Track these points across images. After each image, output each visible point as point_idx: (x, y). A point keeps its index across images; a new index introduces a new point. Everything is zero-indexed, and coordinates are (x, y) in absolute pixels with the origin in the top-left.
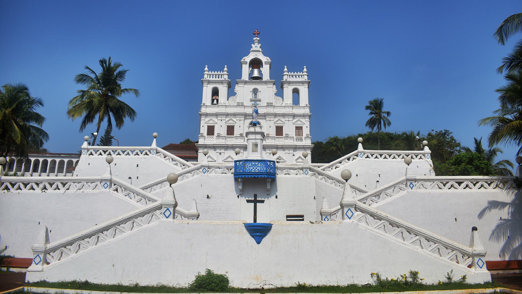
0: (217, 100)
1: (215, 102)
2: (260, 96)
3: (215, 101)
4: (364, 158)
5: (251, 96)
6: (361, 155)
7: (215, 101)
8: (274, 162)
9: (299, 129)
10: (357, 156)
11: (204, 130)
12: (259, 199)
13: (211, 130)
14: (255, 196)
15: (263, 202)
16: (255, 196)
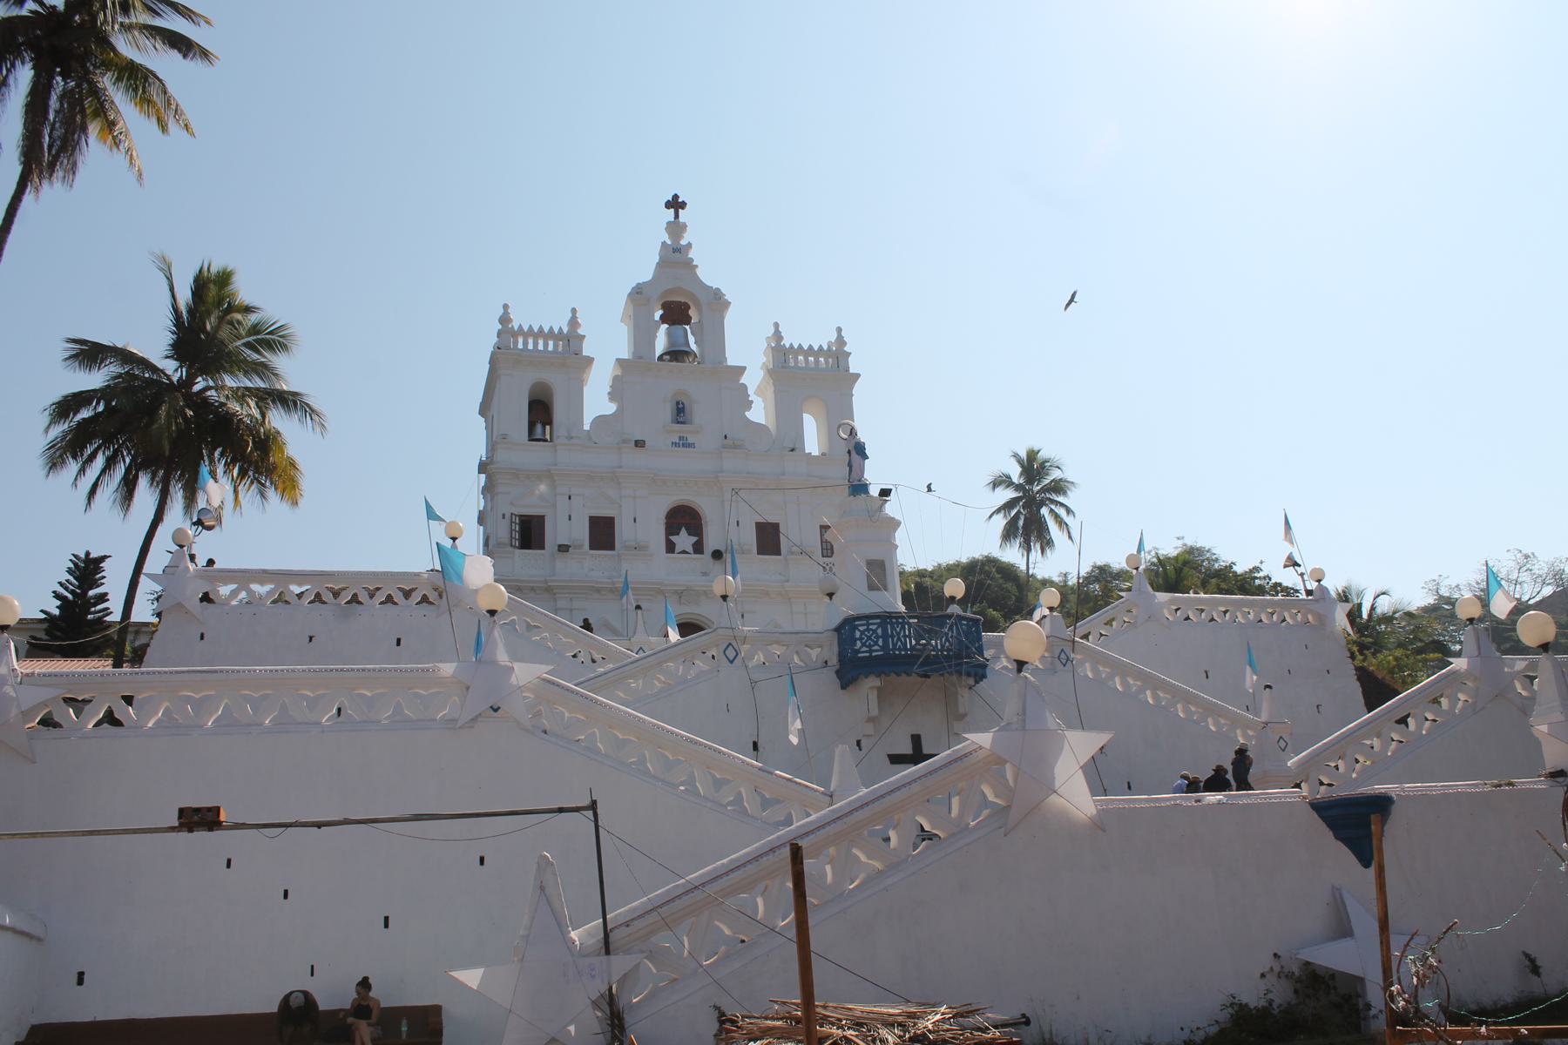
2: (699, 414)
5: (667, 412)
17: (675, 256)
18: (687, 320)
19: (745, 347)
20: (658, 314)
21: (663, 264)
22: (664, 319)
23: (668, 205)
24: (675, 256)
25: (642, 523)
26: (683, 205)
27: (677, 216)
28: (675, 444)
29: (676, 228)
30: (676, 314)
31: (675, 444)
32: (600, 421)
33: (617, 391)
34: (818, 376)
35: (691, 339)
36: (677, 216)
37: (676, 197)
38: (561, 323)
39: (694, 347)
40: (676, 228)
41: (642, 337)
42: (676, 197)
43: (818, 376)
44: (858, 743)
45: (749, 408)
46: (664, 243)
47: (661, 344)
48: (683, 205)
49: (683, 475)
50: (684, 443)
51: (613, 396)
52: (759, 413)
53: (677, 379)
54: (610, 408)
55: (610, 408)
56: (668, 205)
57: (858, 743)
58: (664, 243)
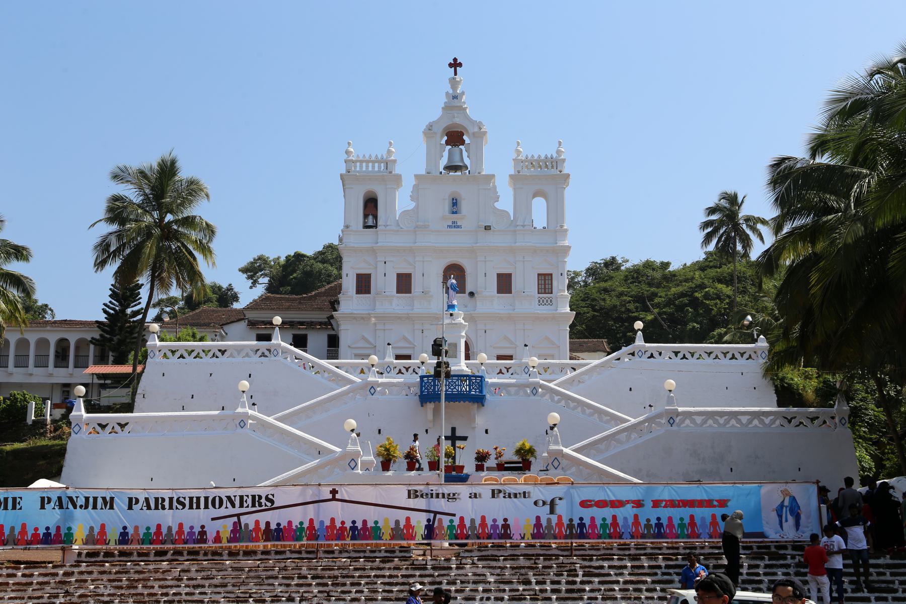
0: (375, 217)
1: (370, 221)
2: (464, 207)
3: (371, 217)
4: (644, 358)
6: (640, 354)
7: (371, 217)
8: (481, 377)
9: (545, 282)
10: (633, 354)
11: (349, 283)
12: (458, 434)
13: (364, 284)
14: (454, 430)
15: (464, 438)
16: (454, 430)
17: (454, 101)
18: (463, 142)
19: (496, 159)
20: (443, 142)
21: (447, 108)
22: (447, 143)
23: (450, 65)
24: (454, 101)
25: (428, 278)
26: (460, 65)
27: (456, 74)
28: (449, 226)
29: (454, 83)
30: (455, 138)
31: (449, 226)
32: (405, 213)
33: (415, 195)
34: (544, 176)
35: (465, 154)
36: (456, 74)
37: (455, 60)
38: (381, 153)
39: (467, 161)
40: (454, 83)
41: (431, 159)
42: (455, 60)
43: (544, 176)
44: (427, 431)
45: (497, 199)
46: (447, 93)
47: (444, 162)
48: (460, 65)
49: (454, 245)
50: (455, 225)
51: (412, 198)
52: (506, 201)
53: (454, 184)
54: (411, 205)
55: (411, 205)
56: (450, 65)
57: (427, 431)
58: (447, 93)
